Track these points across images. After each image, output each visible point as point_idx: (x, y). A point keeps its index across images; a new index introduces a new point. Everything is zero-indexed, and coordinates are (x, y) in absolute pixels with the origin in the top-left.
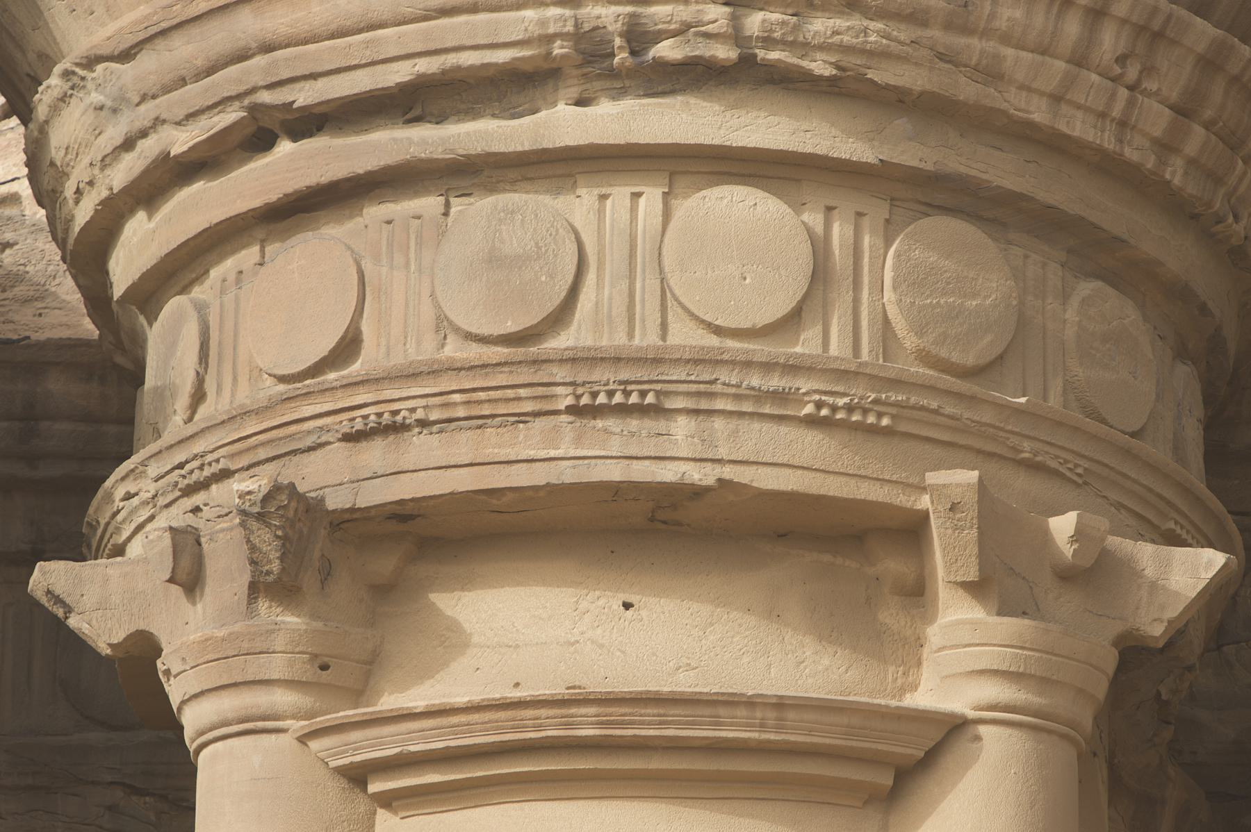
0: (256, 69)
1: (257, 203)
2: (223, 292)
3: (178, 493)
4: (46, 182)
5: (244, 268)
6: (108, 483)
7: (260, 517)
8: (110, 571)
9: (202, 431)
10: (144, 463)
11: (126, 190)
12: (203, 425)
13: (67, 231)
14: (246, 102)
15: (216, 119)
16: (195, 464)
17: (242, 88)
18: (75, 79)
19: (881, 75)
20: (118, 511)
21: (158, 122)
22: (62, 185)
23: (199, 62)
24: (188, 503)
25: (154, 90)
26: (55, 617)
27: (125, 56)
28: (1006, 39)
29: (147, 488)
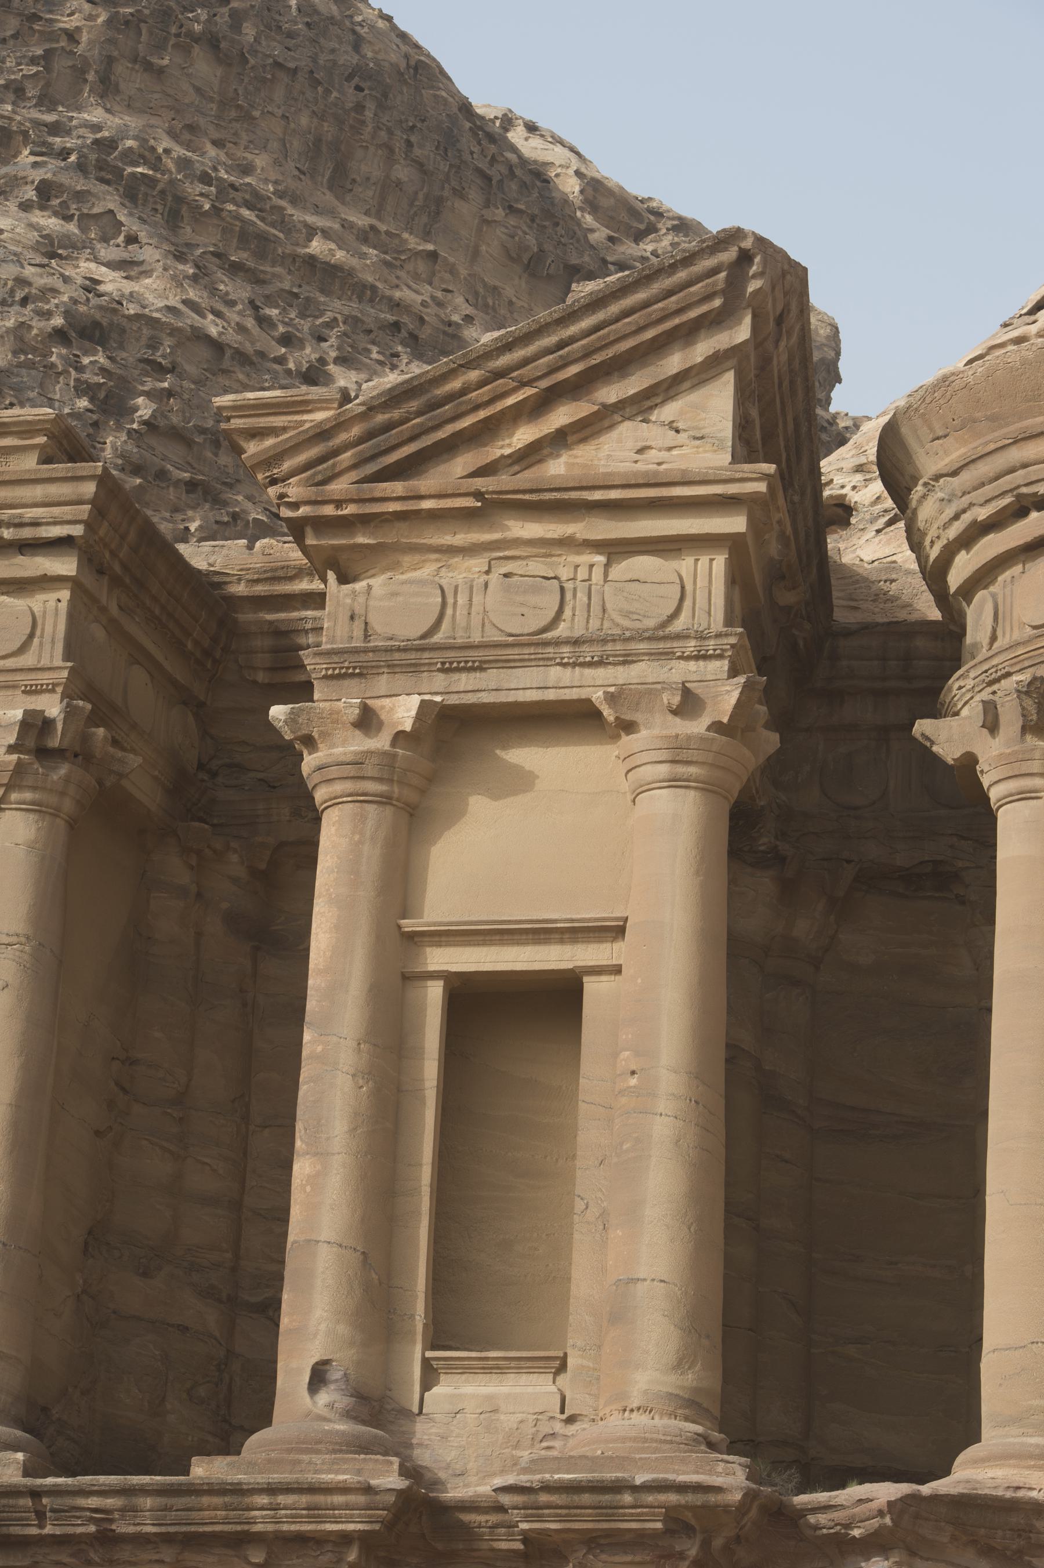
0: (1019, 476)
1: (1021, 542)
2: (1004, 587)
3: (985, 685)
4: (916, 539)
5: (1015, 574)
6: (950, 682)
7: (1027, 693)
8: (953, 723)
9: (997, 654)
10: (968, 671)
11: (956, 540)
12: (997, 651)
13: (927, 561)
14: (1015, 493)
15: (1000, 502)
16: (993, 670)
17: (1013, 486)
18: (930, 487)
20: (955, 696)
21: (971, 505)
22: (924, 540)
23: (991, 475)
24: (990, 689)
25: (969, 490)
26: (926, 747)
27: (954, 473)
29: (969, 683)
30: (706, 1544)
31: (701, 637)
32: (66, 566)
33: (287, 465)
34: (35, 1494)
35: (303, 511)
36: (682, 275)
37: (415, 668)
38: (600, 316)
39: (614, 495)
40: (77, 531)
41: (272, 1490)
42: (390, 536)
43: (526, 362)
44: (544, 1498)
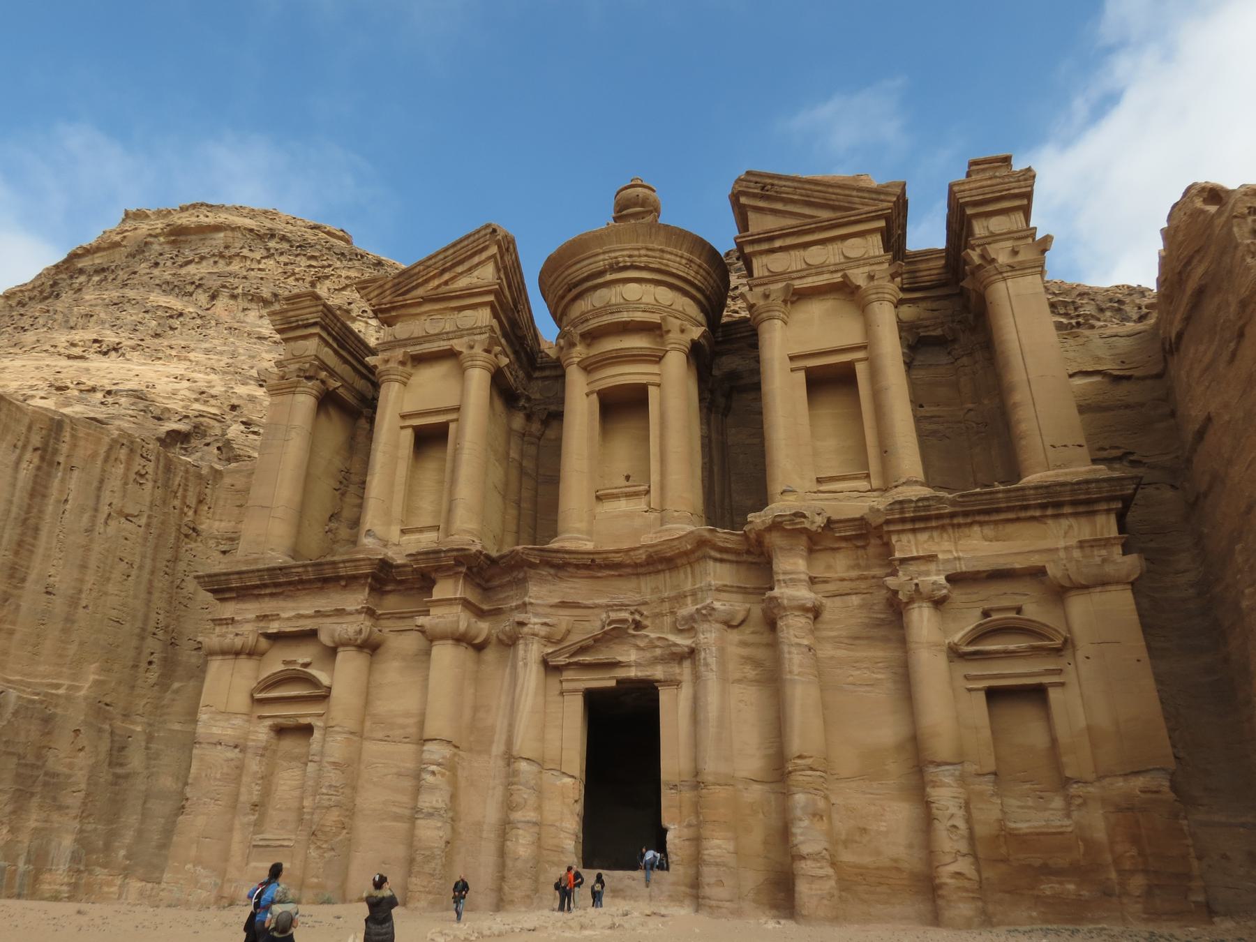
0: (569, 278)
19: (651, 265)
28: (668, 260)
30: (469, 569)
31: (481, 328)
32: (316, 330)
33: (372, 295)
34: (280, 569)
35: (377, 307)
36: (477, 236)
37: (405, 346)
38: (455, 249)
39: (458, 293)
40: (318, 320)
41: (344, 562)
42: (400, 312)
43: (435, 263)
44: (419, 557)
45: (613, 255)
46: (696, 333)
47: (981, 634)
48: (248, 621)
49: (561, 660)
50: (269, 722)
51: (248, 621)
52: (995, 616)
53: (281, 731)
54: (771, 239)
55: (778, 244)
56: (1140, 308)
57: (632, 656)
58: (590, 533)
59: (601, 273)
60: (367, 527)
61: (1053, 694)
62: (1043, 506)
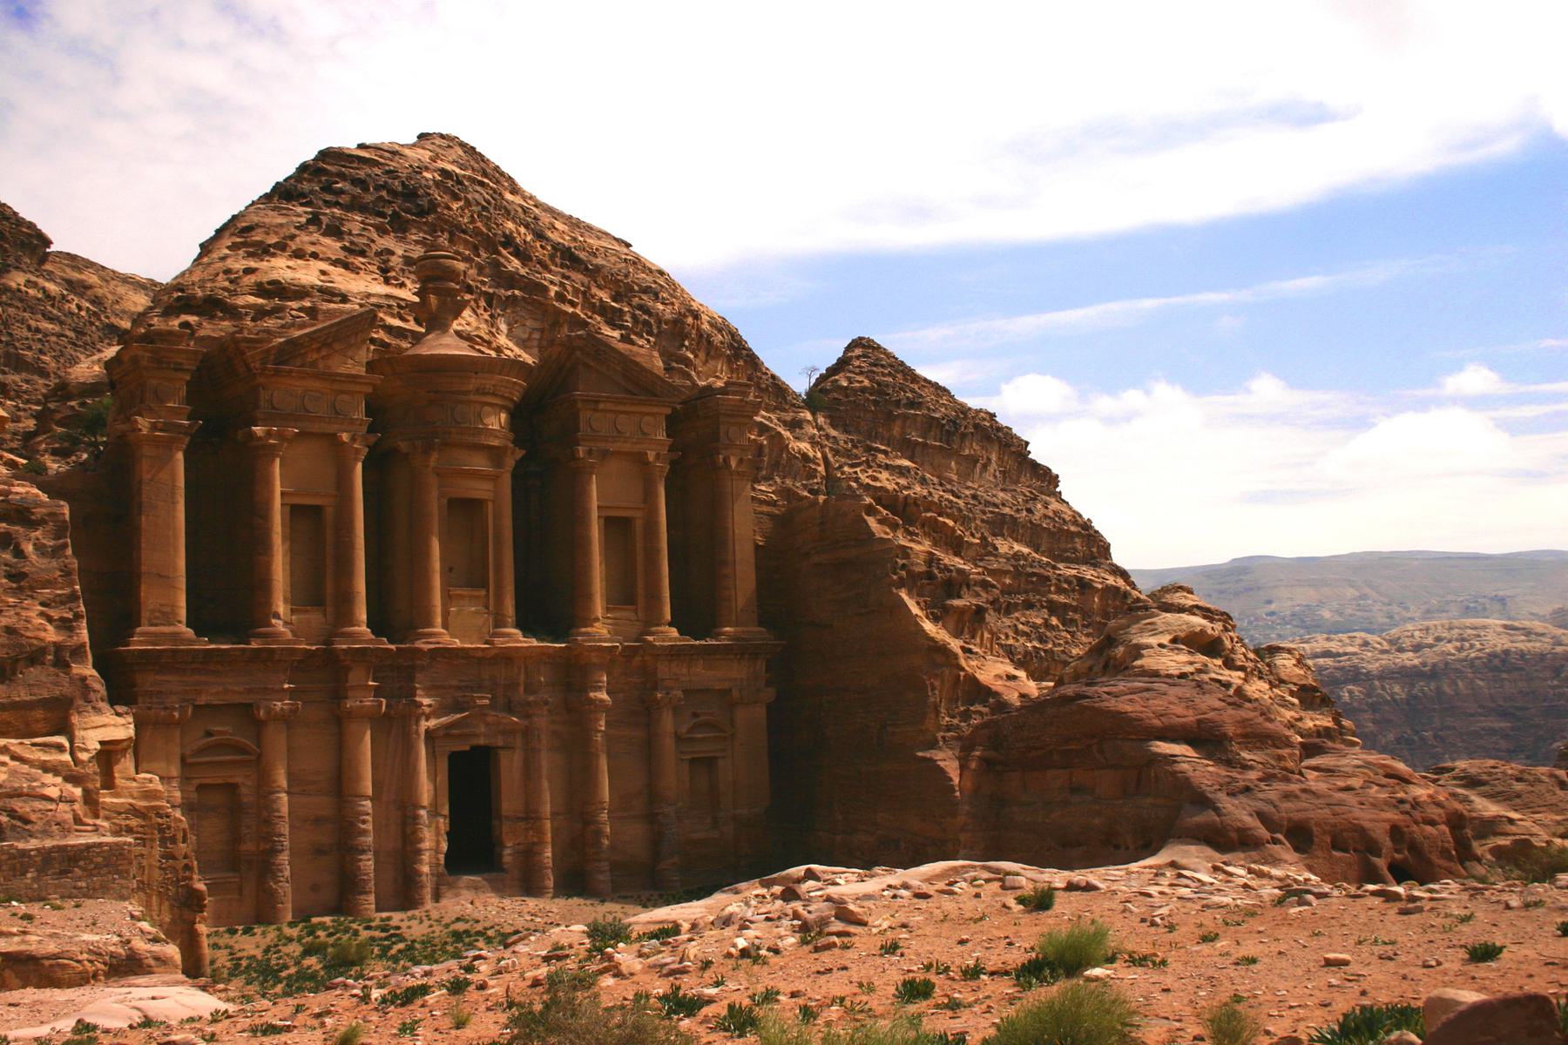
41: (283, 649)
45: (483, 382)
46: (520, 454)
47: (692, 729)
48: (171, 693)
49: (441, 733)
50: (196, 782)
51: (171, 693)
52: (702, 718)
53: (201, 788)
54: (597, 402)
55: (601, 406)
56: (660, 322)
57: (483, 729)
58: (445, 625)
59: (467, 393)
60: (274, 608)
61: (721, 763)
62: (736, 654)
